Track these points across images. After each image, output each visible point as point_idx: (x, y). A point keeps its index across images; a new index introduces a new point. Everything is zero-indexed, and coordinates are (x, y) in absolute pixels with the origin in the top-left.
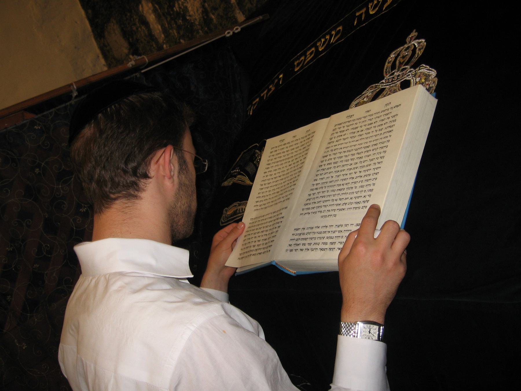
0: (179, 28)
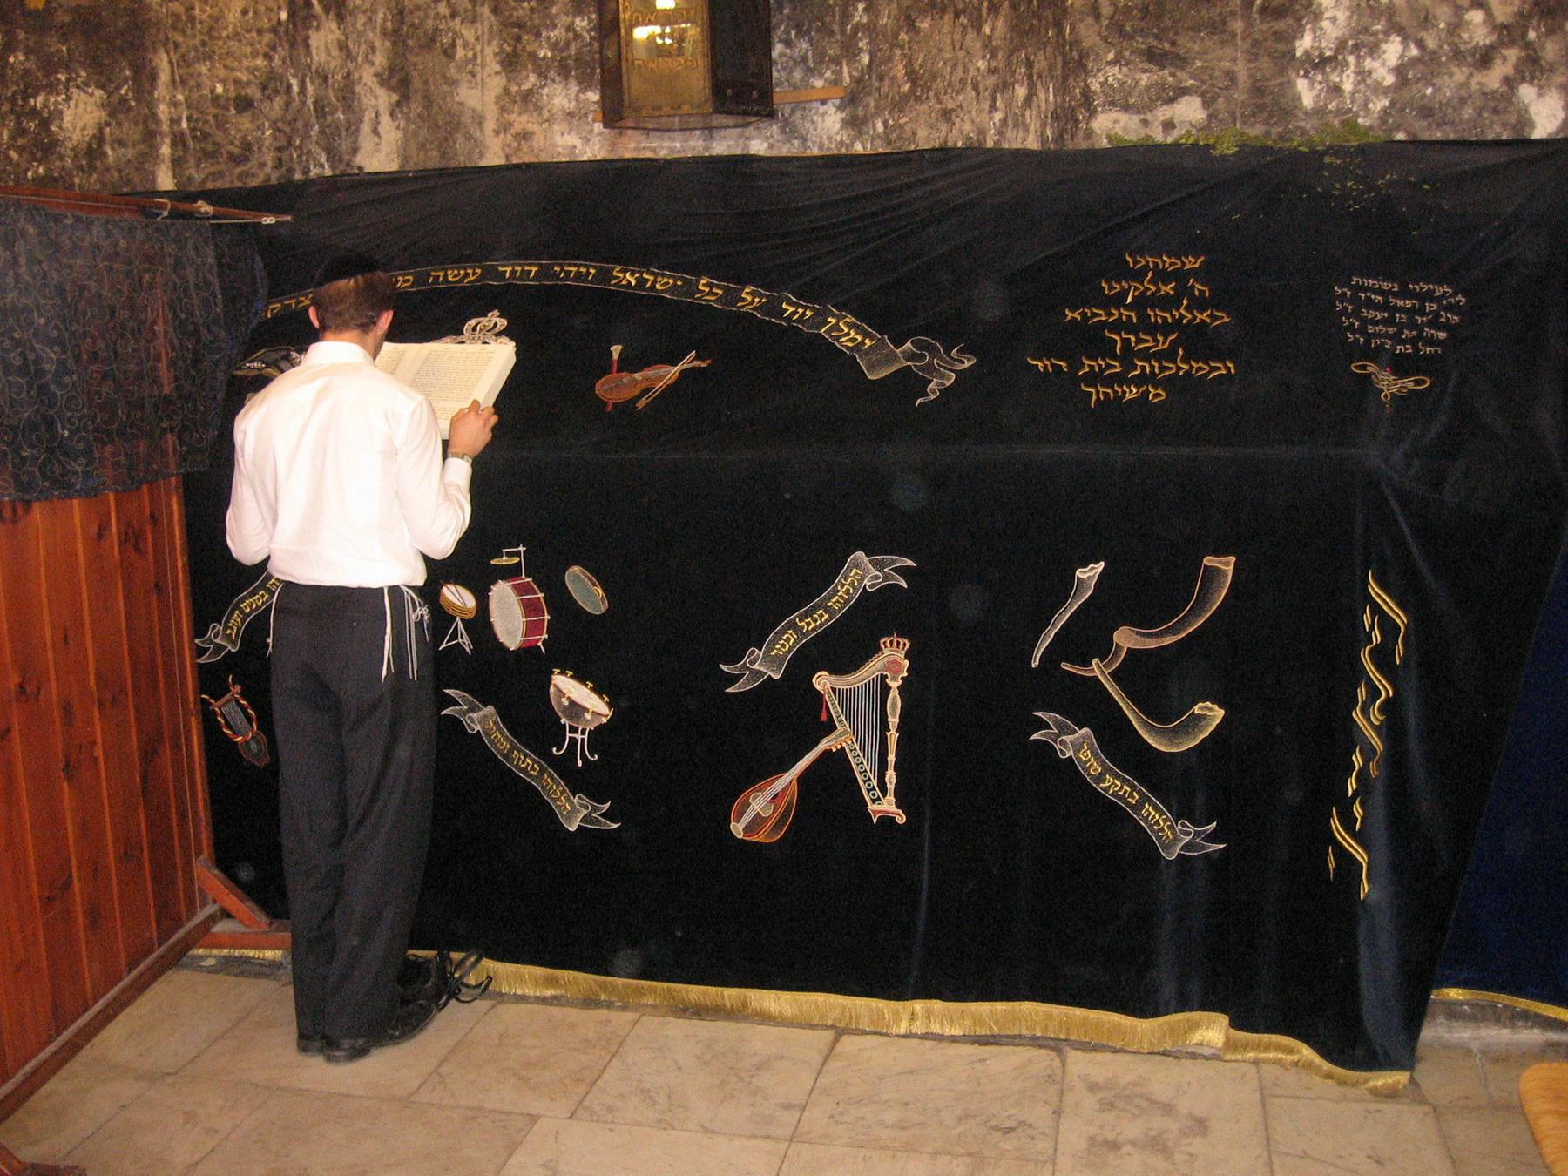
0: (20, 131)
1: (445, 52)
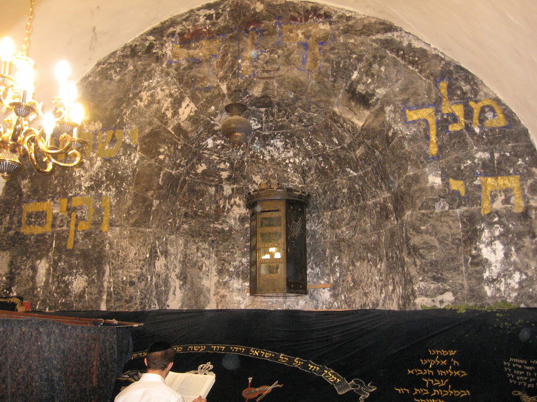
1: (199, 268)
